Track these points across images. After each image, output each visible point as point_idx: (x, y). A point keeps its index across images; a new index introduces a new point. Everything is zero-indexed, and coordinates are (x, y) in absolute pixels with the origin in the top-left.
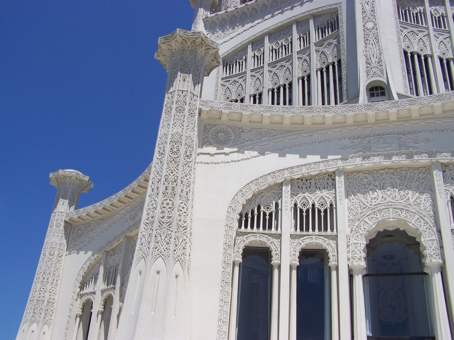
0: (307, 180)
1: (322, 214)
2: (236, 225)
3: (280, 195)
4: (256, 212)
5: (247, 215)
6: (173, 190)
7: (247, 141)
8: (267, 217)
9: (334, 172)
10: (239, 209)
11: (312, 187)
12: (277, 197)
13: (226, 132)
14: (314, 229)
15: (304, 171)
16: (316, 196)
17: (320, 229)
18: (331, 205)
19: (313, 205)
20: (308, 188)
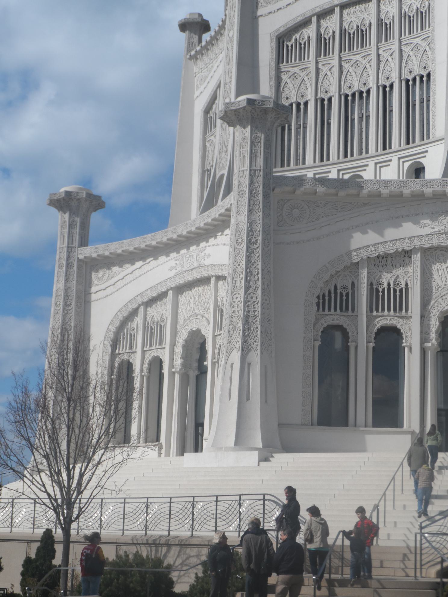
0: (383, 258)
1: (398, 294)
2: (315, 307)
3: (357, 274)
4: (333, 295)
5: (324, 296)
6: (256, 283)
7: (323, 217)
8: (344, 298)
9: (411, 250)
10: (317, 292)
11: (388, 265)
12: (353, 277)
13: (301, 208)
14: (389, 310)
15: (381, 250)
16: (392, 275)
17: (395, 310)
18: (407, 285)
19: (389, 285)
20: (384, 266)
